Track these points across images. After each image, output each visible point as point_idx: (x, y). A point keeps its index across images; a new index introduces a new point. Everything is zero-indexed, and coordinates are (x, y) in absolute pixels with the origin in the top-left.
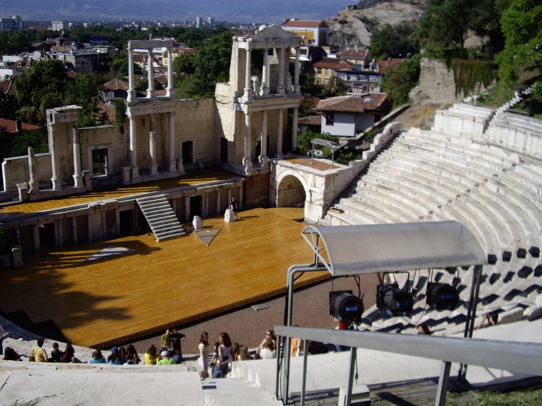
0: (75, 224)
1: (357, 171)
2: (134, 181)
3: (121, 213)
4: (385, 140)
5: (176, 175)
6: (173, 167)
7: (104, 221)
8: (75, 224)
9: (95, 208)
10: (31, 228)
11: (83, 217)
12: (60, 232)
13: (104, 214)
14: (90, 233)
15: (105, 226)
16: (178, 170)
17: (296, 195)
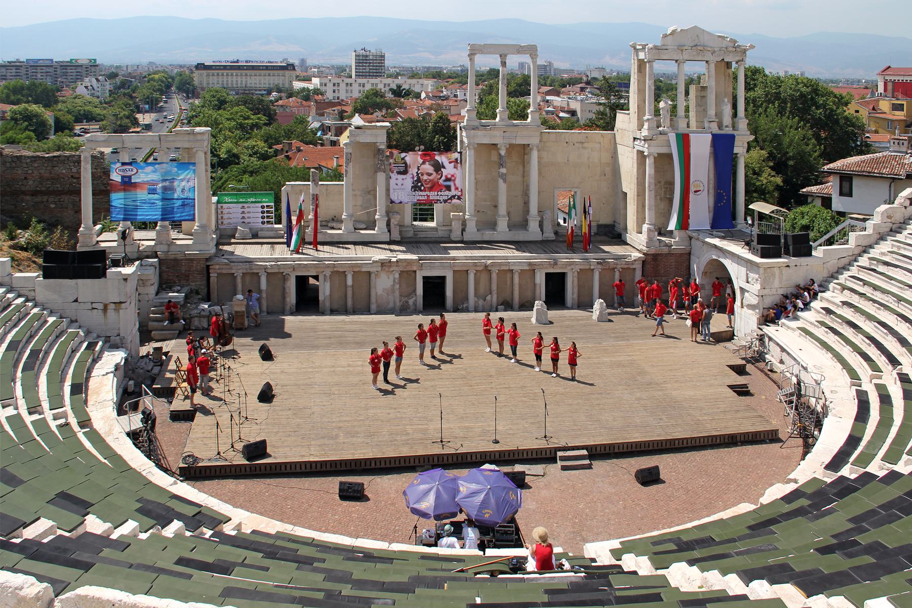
0: (350, 282)
1: (833, 264)
2: (467, 237)
3: (426, 279)
4: (898, 217)
5: (539, 237)
6: (534, 225)
7: (397, 286)
8: (350, 282)
9: (384, 264)
10: (284, 278)
11: (364, 276)
12: (325, 291)
13: (397, 276)
14: (373, 300)
15: (397, 293)
16: (542, 230)
17: (722, 295)
